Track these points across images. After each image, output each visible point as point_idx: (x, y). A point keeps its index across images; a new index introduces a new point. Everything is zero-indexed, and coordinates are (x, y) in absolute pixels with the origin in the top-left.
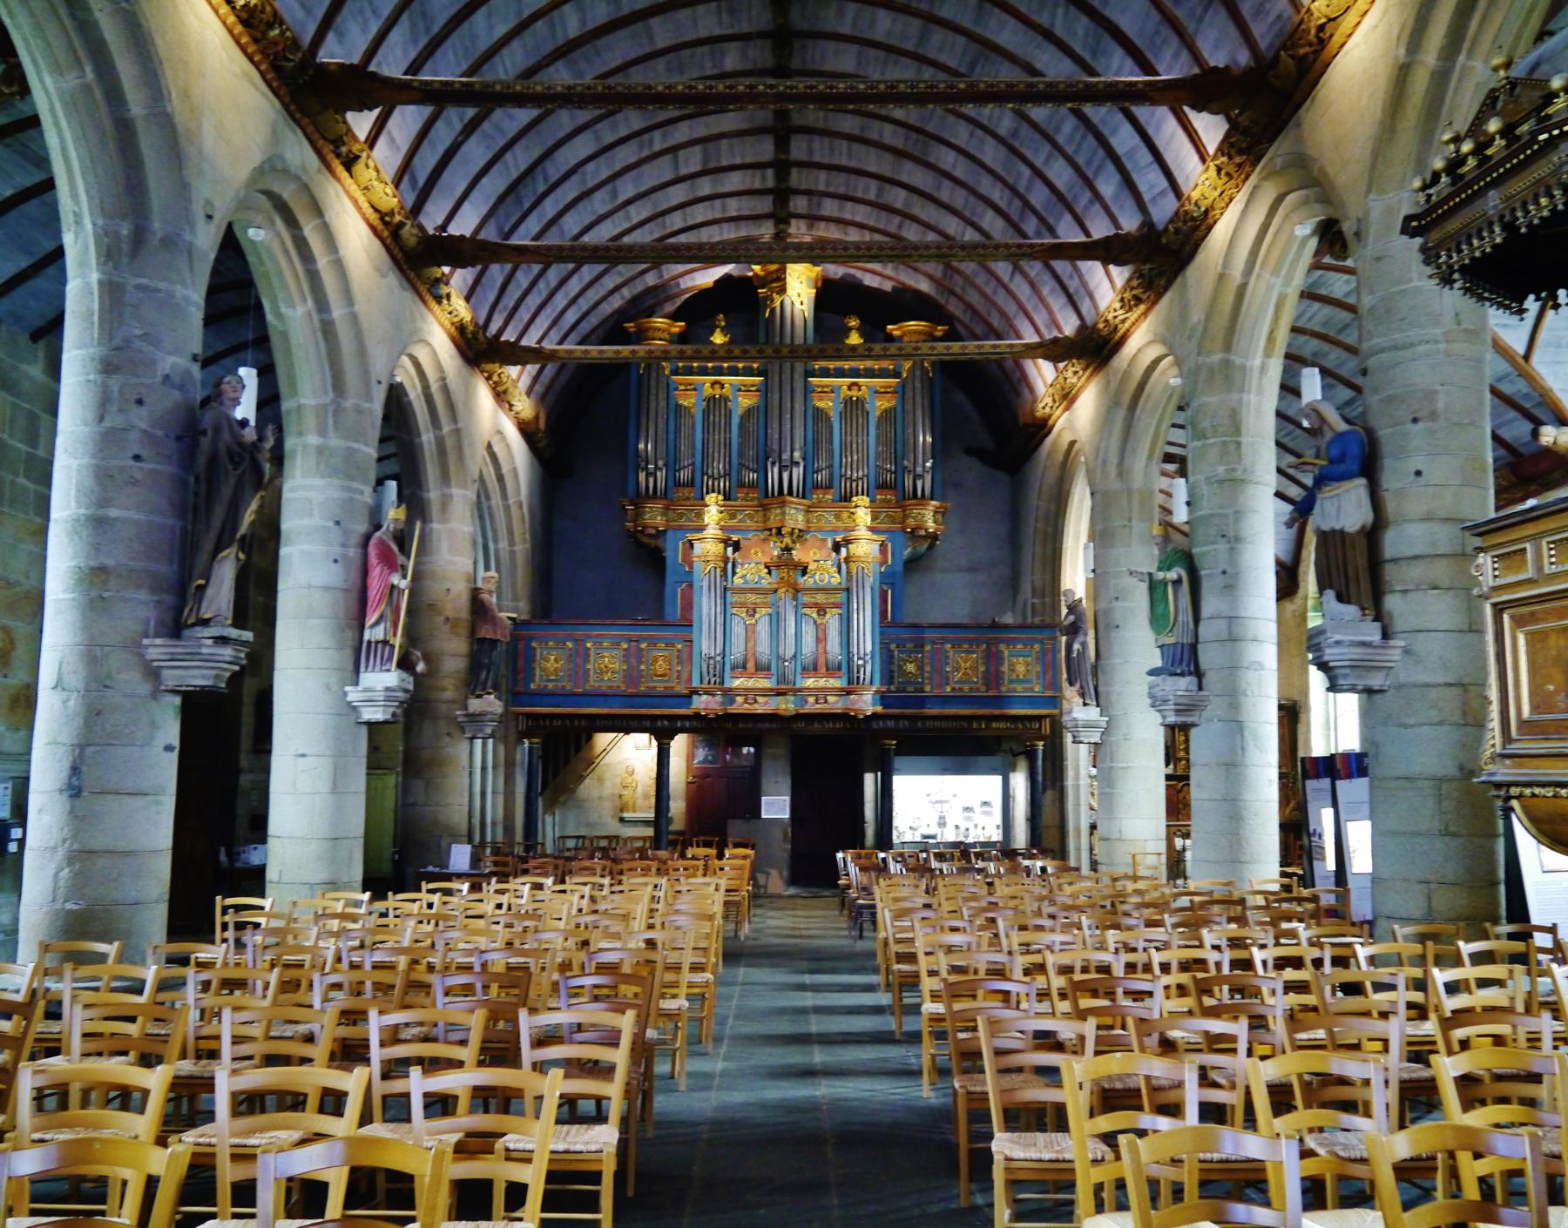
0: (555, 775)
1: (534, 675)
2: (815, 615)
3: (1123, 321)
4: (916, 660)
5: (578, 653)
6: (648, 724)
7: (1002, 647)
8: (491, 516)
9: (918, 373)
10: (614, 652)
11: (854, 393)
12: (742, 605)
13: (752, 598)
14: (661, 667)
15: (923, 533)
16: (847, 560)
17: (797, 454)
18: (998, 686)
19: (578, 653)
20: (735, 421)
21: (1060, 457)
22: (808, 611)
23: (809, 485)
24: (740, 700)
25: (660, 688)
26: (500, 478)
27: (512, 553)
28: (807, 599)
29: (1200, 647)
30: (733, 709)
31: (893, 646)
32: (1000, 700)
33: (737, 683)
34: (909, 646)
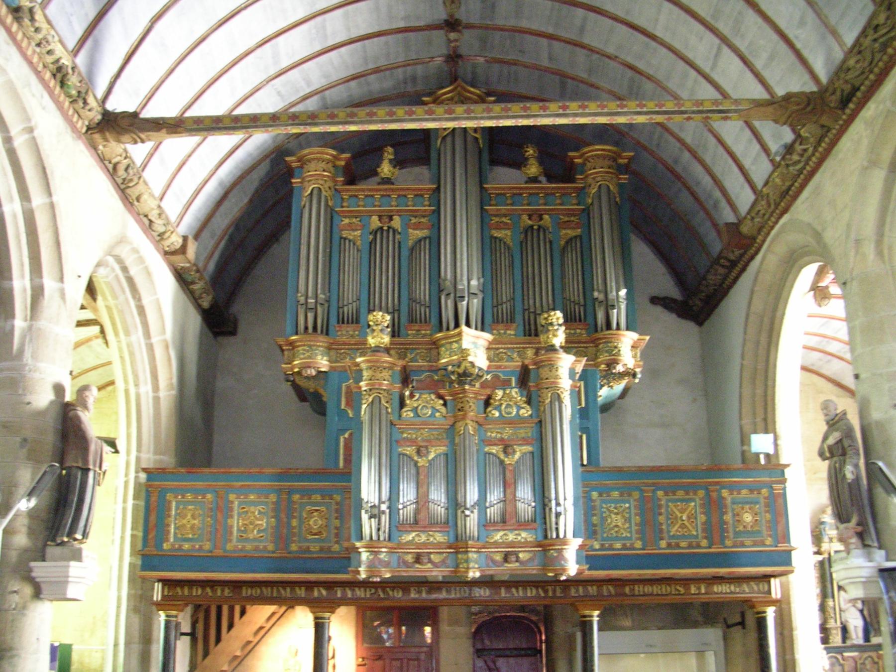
0: (206, 654)
1: (168, 532)
2: (502, 456)
5: (218, 508)
6: (301, 592)
7: (725, 493)
9: (604, 198)
20: (405, 253)
22: (494, 450)
31: (595, 494)
34: (616, 494)
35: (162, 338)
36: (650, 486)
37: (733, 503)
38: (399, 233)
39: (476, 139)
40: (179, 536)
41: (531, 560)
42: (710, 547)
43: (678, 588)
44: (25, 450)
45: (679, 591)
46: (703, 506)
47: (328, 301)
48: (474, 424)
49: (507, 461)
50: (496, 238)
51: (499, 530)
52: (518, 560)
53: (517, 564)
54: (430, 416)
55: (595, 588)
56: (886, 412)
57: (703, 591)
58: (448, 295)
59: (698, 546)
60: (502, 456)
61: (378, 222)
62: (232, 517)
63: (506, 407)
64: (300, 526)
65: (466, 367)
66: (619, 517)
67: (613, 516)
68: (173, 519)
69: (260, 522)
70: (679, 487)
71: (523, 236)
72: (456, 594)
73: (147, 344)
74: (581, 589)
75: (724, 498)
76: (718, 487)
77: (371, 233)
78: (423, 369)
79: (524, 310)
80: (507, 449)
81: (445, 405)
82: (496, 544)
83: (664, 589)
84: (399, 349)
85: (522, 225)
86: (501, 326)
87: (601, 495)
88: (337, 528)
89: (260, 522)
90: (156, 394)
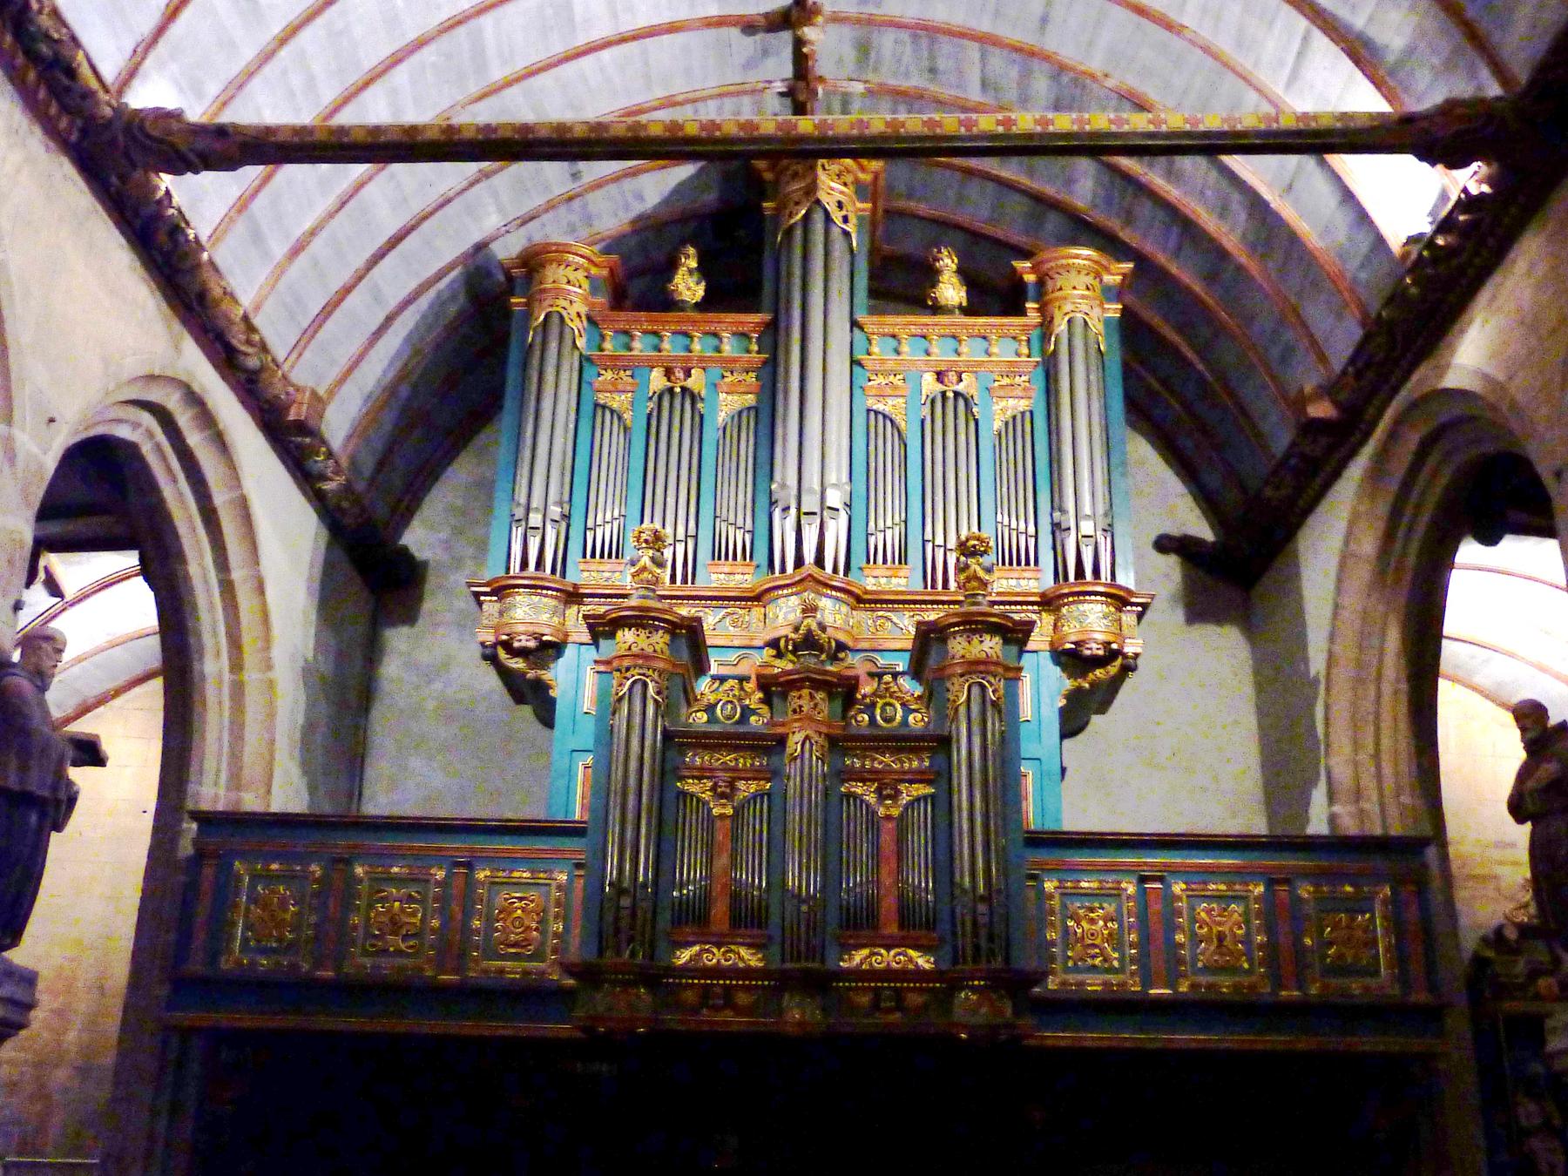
1: (232, 938)
2: (871, 798)
20: (710, 435)
22: (859, 789)
23: (858, 559)
39: (846, 234)
47: (567, 517)
48: (821, 740)
49: (881, 811)
50: (876, 413)
52: (900, 1007)
53: (898, 1015)
54: (737, 723)
58: (786, 509)
60: (871, 798)
63: (883, 709)
64: (489, 929)
71: (926, 411)
77: (651, 398)
79: (924, 542)
80: (887, 786)
81: (767, 701)
82: (857, 974)
90: (235, 677)
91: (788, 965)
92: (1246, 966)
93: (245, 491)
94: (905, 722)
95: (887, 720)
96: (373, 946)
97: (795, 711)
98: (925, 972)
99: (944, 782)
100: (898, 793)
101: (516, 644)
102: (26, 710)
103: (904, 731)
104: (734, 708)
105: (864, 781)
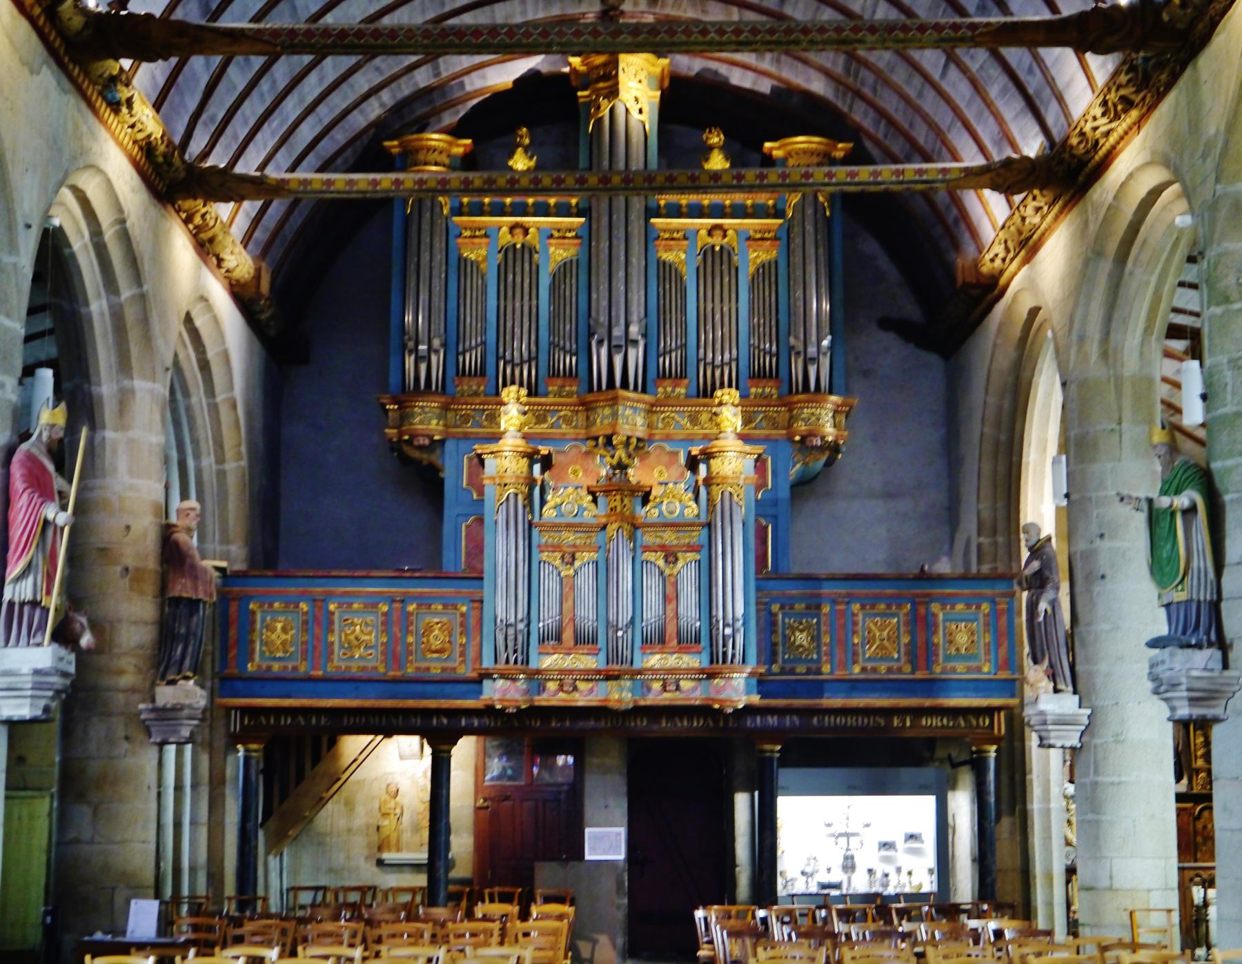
1: (253, 651)
2: (661, 563)
3: (1107, 134)
4: (808, 628)
5: (316, 620)
8: (191, 418)
9: (810, 211)
10: (369, 618)
11: (717, 240)
12: (556, 548)
13: (570, 538)
14: (437, 638)
15: (817, 442)
16: (708, 482)
17: (634, 330)
18: (929, 662)
19: (316, 620)
21: (1016, 332)
22: (650, 556)
24: (552, 686)
25: (436, 670)
26: (204, 366)
27: (221, 474)
28: (648, 538)
29: (1223, 605)
30: (543, 700)
31: (775, 608)
32: (932, 686)
33: (548, 662)
35: (229, 395)
36: (844, 597)
37: (945, 621)
38: (537, 252)
40: (267, 654)
41: (695, 689)
42: (913, 672)
43: (877, 719)
44: (127, 580)
45: (879, 724)
46: (907, 624)
49: (667, 572)
51: (655, 653)
52: (678, 688)
54: (576, 515)
55: (775, 718)
56: (1092, 542)
57: (908, 724)
59: (900, 670)
61: (509, 237)
62: (332, 631)
65: (620, 459)
66: (805, 634)
67: (797, 634)
68: (257, 633)
69: (366, 638)
70: (878, 598)
72: (606, 723)
73: (209, 405)
74: (758, 719)
75: (935, 616)
76: (927, 599)
77: (500, 252)
78: (567, 437)
79: (698, 361)
81: (595, 501)
82: (653, 671)
83: (860, 720)
84: (537, 410)
85: (700, 245)
86: (667, 382)
87: (782, 607)
88: (461, 645)
89: (366, 638)
91: (611, 667)
92: (896, 656)
93: (227, 346)
94: (682, 513)
95: (671, 513)
96: (344, 654)
97: (612, 509)
98: (692, 669)
99: (705, 551)
100: (677, 559)
101: (416, 443)
102: (191, 552)
103: (681, 520)
104: (573, 506)
105: (656, 551)
